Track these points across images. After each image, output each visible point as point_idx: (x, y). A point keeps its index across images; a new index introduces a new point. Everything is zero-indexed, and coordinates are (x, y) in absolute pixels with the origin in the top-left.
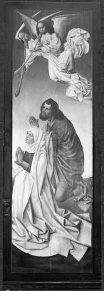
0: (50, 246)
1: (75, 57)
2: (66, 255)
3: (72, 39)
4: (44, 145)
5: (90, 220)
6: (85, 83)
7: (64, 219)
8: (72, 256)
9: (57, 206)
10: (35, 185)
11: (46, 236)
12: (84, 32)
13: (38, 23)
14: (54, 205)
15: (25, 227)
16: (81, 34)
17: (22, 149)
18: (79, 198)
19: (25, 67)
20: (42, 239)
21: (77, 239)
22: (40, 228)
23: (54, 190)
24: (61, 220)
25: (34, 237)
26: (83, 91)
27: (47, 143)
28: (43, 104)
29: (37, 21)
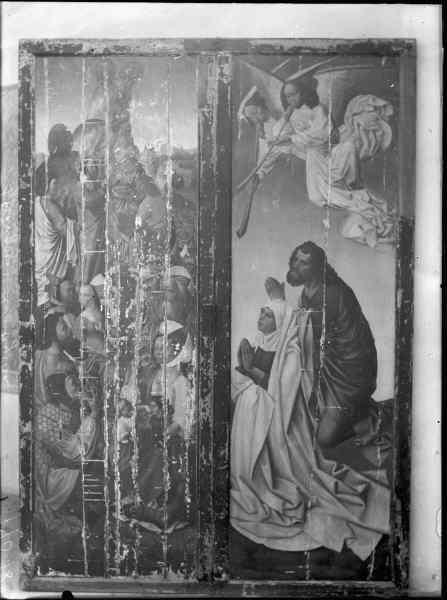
0: (308, 531)
1: (361, 156)
2: (338, 548)
3: (355, 117)
4: (297, 334)
5: (386, 482)
6: (382, 211)
7: (335, 480)
8: (350, 550)
9: (321, 456)
10: (278, 414)
11: (299, 514)
12: (381, 102)
13: (285, 83)
14: (316, 452)
15: (254, 492)
16: (376, 108)
17: (251, 343)
18: (366, 440)
19: (256, 176)
20: (291, 518)
21: (363, 516)
22: (288, 497)
23: (315, 424)
24: (330, 482)
25: (274, 513)
26: (377, 227)
27: (302, 331)
28: (295, 253)
29: (282, 80)
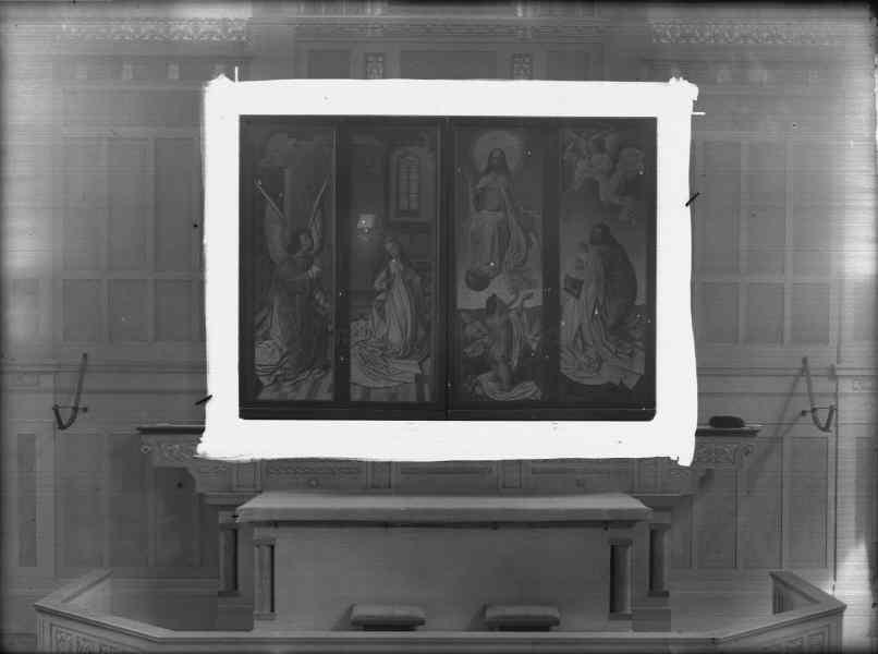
2: (617, 382)
